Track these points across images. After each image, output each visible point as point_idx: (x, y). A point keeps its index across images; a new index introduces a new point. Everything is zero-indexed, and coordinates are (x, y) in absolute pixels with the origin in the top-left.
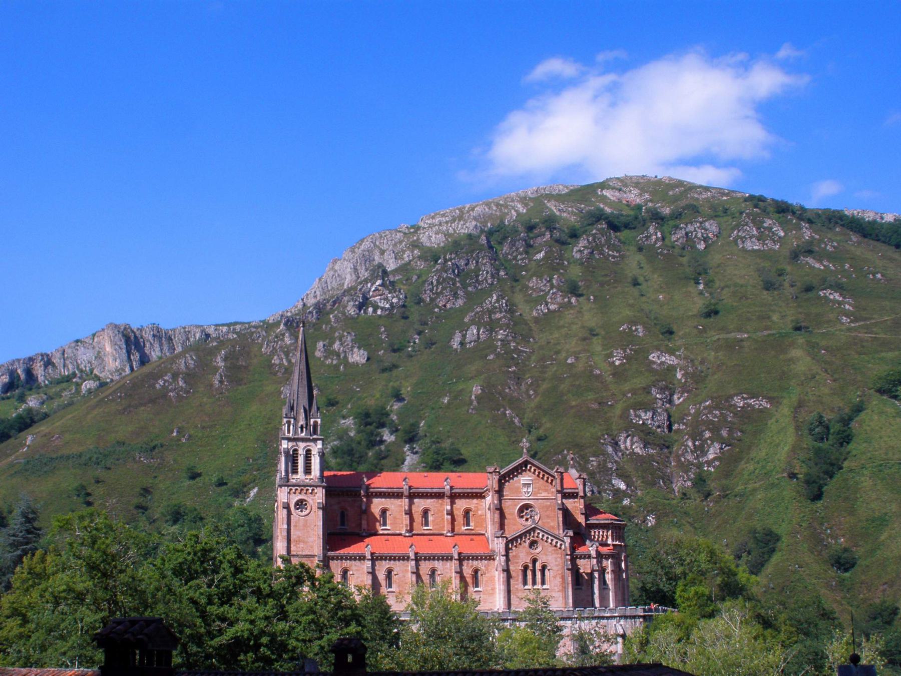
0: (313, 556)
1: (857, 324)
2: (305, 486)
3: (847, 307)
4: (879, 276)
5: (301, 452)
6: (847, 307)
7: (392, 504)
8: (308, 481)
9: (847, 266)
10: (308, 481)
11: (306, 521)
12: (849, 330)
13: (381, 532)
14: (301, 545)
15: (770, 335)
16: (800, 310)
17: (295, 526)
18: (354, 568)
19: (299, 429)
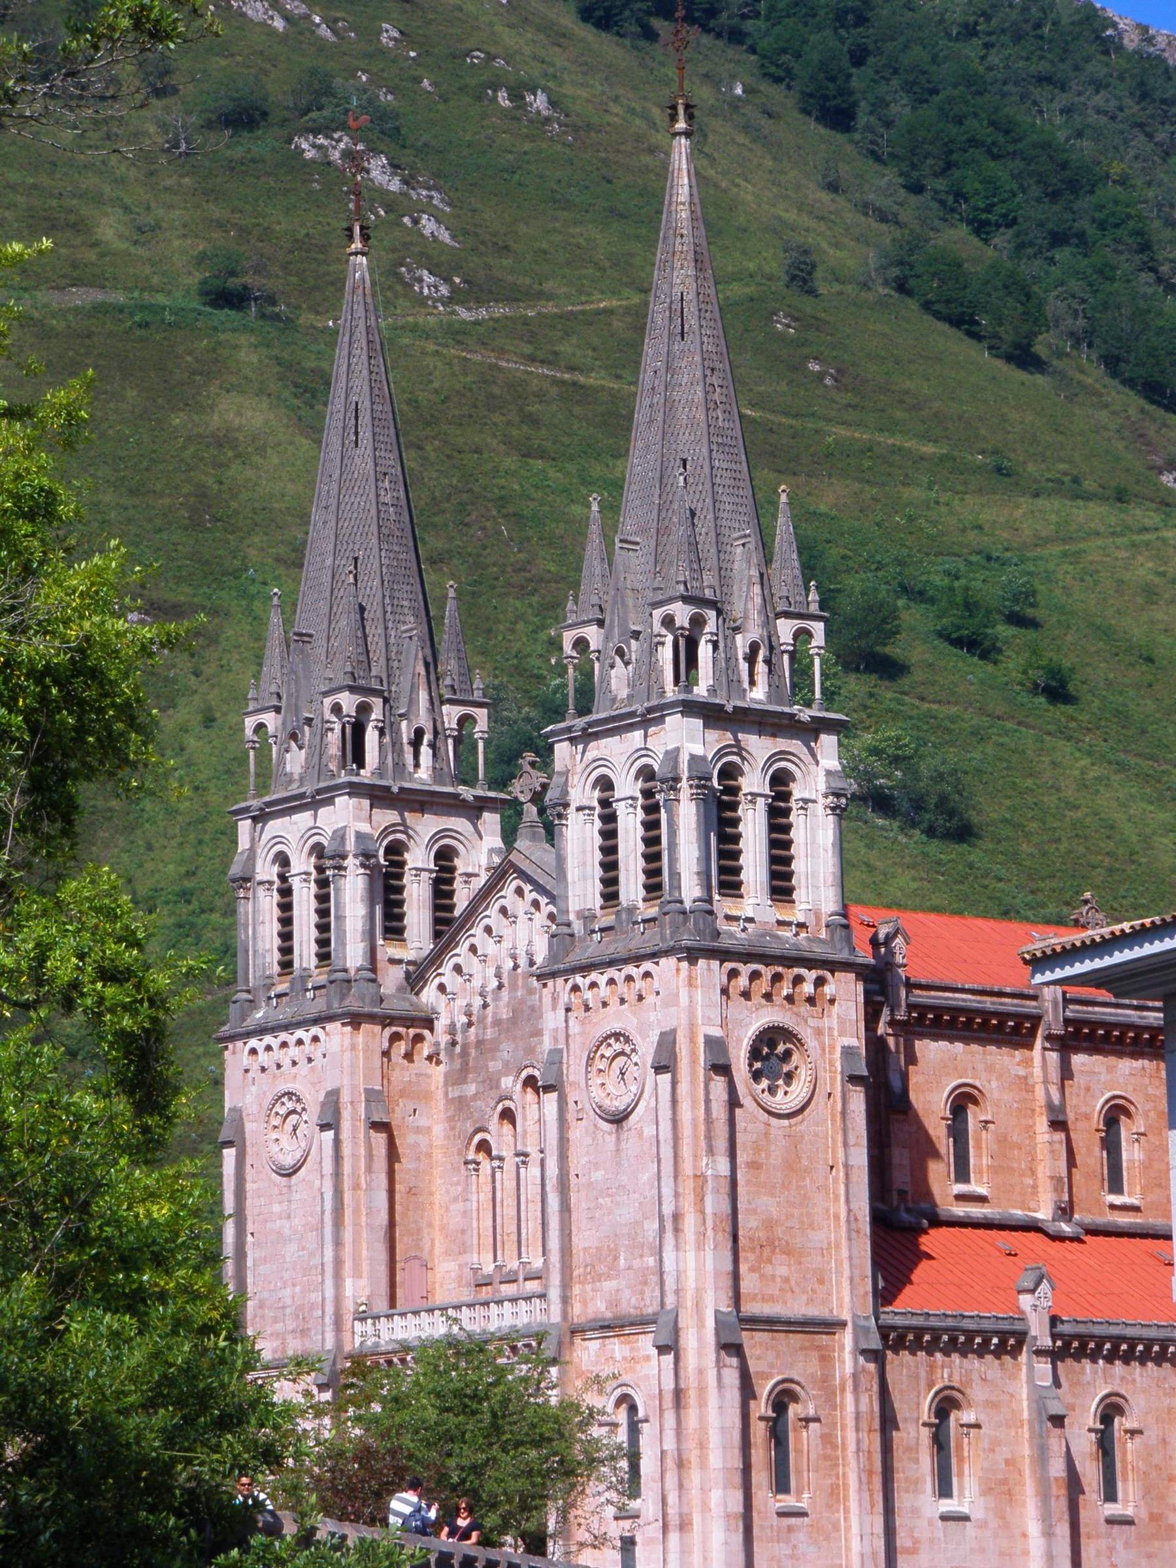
0: (831, 1326)
1: (483, 313)
2: (790, 961)
3: (428, 225)
4: (539, 102)
5: (753, 781)
6: (428, 225)
7: (990, 1069)
8: (787, 934)
9: (389, 34)
10: (787, 934)
11: (795, 1141)
12: (457, 334)
13: (960, 1210)
14: (781, 1268)
15: (100, 309)
16: (217, 212)
17: (754, 1166)
18: (977, 1393)
19: (744, 666)
